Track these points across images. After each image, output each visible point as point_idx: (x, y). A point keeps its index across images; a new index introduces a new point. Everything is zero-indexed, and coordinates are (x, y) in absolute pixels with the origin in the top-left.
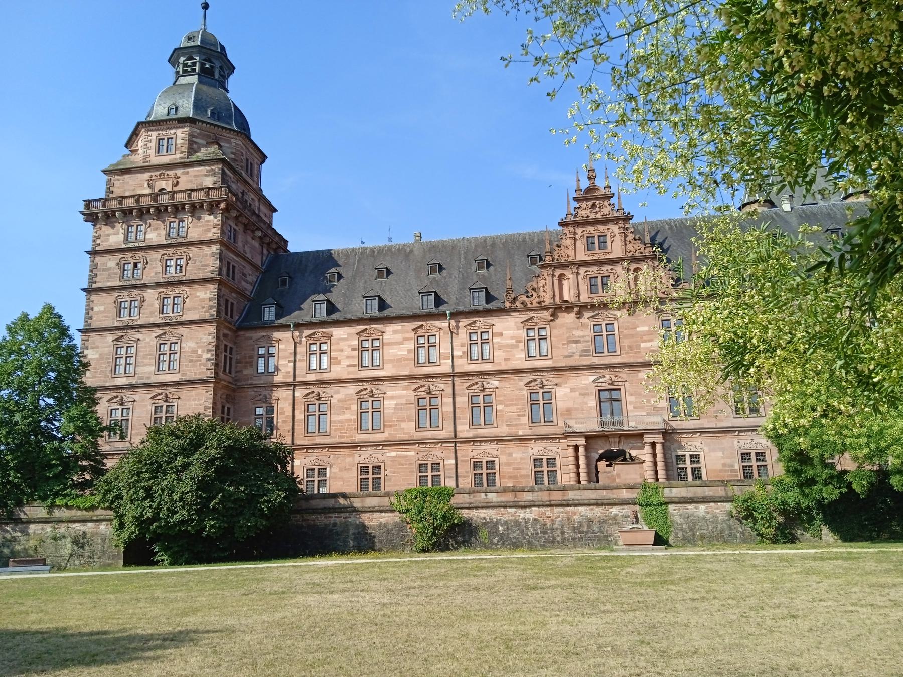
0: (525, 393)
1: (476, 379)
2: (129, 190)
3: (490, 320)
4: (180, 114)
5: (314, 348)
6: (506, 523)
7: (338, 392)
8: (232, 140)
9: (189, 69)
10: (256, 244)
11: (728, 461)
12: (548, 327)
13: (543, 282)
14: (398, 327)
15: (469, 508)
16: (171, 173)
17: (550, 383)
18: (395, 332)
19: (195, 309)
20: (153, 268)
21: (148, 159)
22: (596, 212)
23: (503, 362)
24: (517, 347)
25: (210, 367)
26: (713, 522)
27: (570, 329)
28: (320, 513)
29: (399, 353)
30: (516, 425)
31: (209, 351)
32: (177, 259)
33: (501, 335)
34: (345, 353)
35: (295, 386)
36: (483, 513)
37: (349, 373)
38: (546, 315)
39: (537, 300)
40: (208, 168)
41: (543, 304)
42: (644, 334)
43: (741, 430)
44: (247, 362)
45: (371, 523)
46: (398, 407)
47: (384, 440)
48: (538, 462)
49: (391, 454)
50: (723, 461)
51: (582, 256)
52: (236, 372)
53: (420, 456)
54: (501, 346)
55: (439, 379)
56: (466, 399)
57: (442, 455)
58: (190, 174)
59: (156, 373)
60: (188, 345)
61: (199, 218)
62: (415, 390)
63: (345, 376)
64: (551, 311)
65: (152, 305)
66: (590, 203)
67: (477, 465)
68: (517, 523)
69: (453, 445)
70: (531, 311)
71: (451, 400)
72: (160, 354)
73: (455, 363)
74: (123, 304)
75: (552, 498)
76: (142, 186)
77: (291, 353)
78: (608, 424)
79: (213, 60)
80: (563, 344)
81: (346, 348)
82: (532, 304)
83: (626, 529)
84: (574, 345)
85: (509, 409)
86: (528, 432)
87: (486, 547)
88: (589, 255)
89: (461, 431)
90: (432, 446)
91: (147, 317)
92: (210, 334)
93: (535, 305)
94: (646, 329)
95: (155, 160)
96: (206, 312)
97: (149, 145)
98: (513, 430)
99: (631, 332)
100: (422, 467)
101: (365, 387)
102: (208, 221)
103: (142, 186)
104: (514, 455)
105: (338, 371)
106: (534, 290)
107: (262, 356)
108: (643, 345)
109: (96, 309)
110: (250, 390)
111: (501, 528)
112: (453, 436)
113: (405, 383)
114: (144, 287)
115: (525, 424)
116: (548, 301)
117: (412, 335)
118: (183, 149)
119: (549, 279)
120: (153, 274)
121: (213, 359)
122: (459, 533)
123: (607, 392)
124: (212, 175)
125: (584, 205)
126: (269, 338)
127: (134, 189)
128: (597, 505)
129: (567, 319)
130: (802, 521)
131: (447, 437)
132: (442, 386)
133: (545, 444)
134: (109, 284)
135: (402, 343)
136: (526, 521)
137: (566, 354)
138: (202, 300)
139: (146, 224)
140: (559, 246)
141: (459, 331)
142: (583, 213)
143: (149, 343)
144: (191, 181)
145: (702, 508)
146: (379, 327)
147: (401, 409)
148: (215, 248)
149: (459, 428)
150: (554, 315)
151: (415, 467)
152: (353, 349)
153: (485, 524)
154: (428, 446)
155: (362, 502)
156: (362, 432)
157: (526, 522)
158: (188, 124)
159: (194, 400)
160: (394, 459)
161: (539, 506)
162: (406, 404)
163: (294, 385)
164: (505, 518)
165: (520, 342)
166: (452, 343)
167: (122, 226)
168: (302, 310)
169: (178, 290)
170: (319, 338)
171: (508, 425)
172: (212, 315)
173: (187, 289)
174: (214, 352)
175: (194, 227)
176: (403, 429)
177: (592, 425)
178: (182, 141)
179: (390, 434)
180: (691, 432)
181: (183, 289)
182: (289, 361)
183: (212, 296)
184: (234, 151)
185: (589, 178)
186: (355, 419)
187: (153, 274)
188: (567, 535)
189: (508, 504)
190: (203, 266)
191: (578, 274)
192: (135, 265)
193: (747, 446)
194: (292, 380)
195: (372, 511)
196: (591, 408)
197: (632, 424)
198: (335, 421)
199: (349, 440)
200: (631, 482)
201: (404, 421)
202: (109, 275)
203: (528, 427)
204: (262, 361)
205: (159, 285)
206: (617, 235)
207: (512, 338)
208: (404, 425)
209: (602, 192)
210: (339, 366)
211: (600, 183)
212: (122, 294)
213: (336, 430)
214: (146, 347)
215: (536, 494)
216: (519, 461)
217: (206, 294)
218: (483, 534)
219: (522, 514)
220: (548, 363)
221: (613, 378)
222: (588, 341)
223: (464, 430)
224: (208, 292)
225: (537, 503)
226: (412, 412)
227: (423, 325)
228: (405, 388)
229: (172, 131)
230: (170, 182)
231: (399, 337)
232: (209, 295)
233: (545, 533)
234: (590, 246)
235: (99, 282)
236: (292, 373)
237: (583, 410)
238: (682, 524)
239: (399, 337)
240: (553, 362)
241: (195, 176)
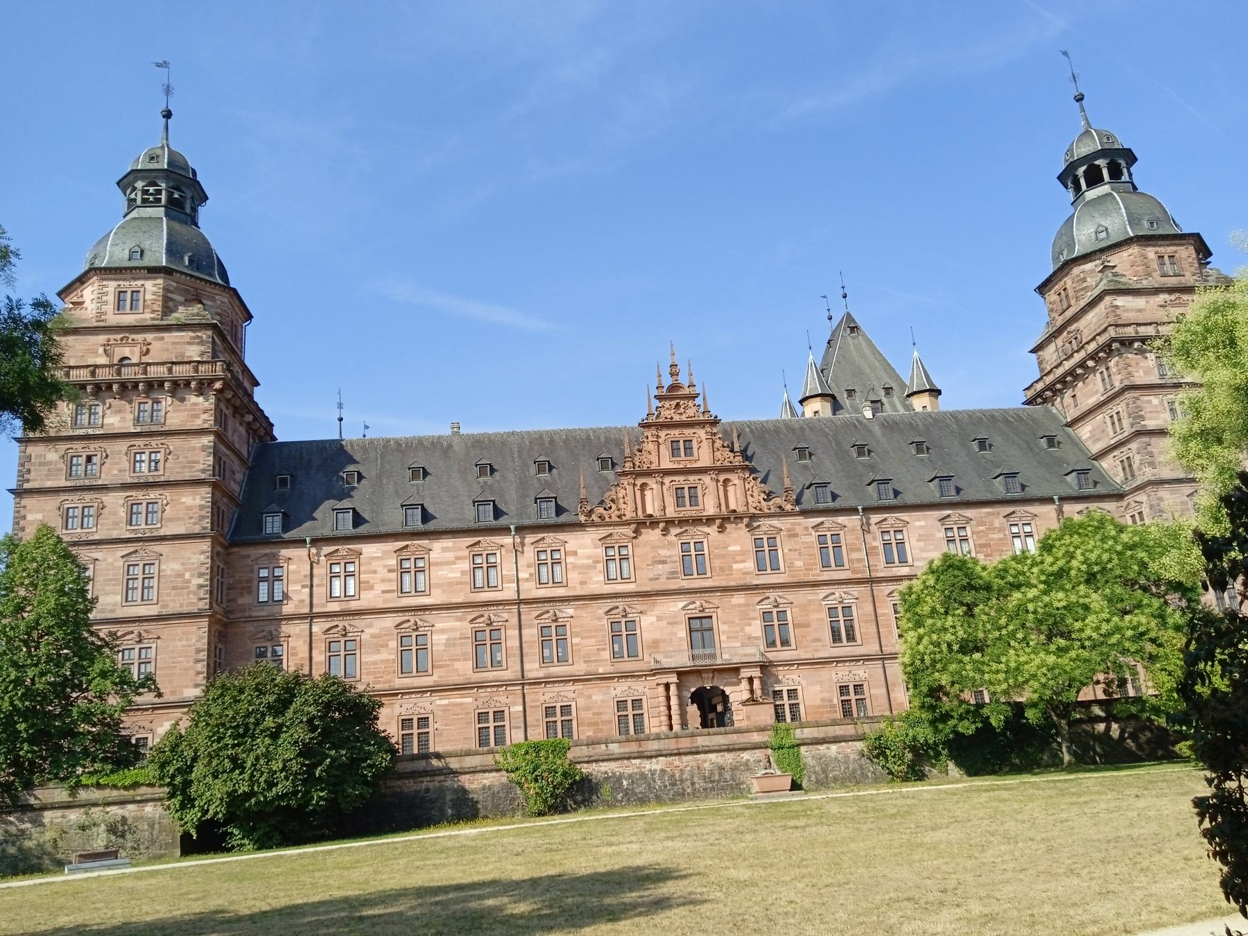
0: (605, 623)
1: (547, 607)
2: (75, 357)
3: (562, 536)
4: (149, 261)
5: (336, 569)
6: (630, 776)
7: (371, 626)
8: (217, 297)
9: (151, 198)
10: (242, 430)
11: (827, 695)
12: (630, 545)
13: (623, 491)
14: (448, 543)
15: (588, 762)
16: (139, 337)
17: (634, 611)
18: (445, 550)
19: (179, 519)
20: (116, 463)
21: (103, 317)
22: (681, 414)
23: (578, 586)
24: (595, 568)
25: (202, 596)
26: (845, 763)
27: (655, 548)
28: (407, 778)
29: (451, 575)
30: (596, 661)
31: (201, 575)
32: (151, 453)
33: (575, 553)
34: (379, 576)
35: (312, 618)
36: (605, 767)
37: (385, 601)
38: (628, 531)
39: (617, 513)
40: (191, 334)
41: (624, 518)
42: (736, 553)
43: (839, 661)
44: (242, 588)
45: (473, 786)
46: (450, 644)
47: (432, 684)
48: (622, 705)
49: (442, 701)
50: (821, 696)
51: (667, 464)
52: (229, 601)
53: (480, 703)
54: (575, 567)
55: (501, 607)
56: (535, 631)
57: (507, 701)
58: (166, 340)
59: (124, 604)
60: (170, 567)
61: (182, 400)
62: (472, 621)
63: (380, 605)
64: (633, 526)
65: (115, 514)
66: (674, 403)
67: (550, 711)
68: (643, 776)
69: (520, 687)
70: (610, 525)
71: (517, 632)
72: (128, 579)
73: (521, 588)
74: (71, 511)
75: (680, 746)
76: (95, 352)
77: (305, 576)
78: (699, 657)
79: (184, 189)
80: (648, 565)
81: (380, 569)
82: (610, 517)
83: (758, 775)
84: (660, 566)
85: (586, 642)
86: (610, 669)
87: (611, 806)
88: (674, 462)
89: (530, 671)
90: (494, 689)
91: (108, 529)
92: (203, 552)
93: (615, 519)
94: (737, 548)
95: (113, 319)
96: (195, 524)
97: (104, 298)
98: (592, 668)
99: (722, 552)
100: (482, 717)
101: (407, 618)
102: (195, 404)
103: (95, 352)
104: (594, 698)
105: (369, 599)
106: (613, 501)
107: (264, 579)
108: (735, 566)
109: (30, 517)
110: (248, 624)
111: (625, 783)
112: (520, 676)
113: (459, 613)
114: (104, 488)
115: (606, 660)
116: (629, 515)
117: (466, 553)
118: (155, 307)
119: (630, 488)
120: (116, 472)
121: (206, 586)
122: (577, 791)
123: (698, 621)
124: (198, 344)
125: (667, 404)
126: (275, 557)
127: (83, 356)
128: (729, 750)
129: (651, 536)
130: (930, 757)
131: (512, 678)
132: (506, 616)
133: (630, 683)
134: (49, 484)
135: (454, 563)
136: (653, 772)
137: (652, 576)
138: (189, 508)
139: (104, 404)
140: (640, 451)
141: (525, 548)
142: (666, 413)
143: (112, 564)
144: (167, 350)
145: (834, 748)
146: (425, 542)
147: (454, 645)
148: (208, 440)
149: (527, 666)
150: (637, 531)
151: (473, 717)
152: (390, 571)
153: (607, 779)
154: (489, 690)
155: (460, 761)
156: (404, 675)
157: (652, 775)
158: (162, 275)
159: (181, 640)
160: (445, 709)
161: (666, 756)
162: (460, 638)
163: (311, 617)
164: (629, 771)
165: (598, 562)
166: (516, 563)
167: (68, 406)
168: (314, 519)
169: (153, 494)
170: (343, 557)
171: (585, 662)
172: (205, 528)
173: (168, 494)
174: (208, 577)
175: (175, 411)
176: (457, 670)
177: (683, 660)
178: (154, 297)
179: (439, 677)
180: (789, 664)
181: (161, 492)
182: (303, 587)
183: (203, 502)
184: (219, 311)
185: (672, 375)
186: (393, 660)
187: (116, 472)
188: (697, 786)
189: (633, 755)
190: (188, 462)
191: (662, 483)
192: (89, 459)
193: (846, 678)
194: (307, 610)
195: (473, 771)
196: (680, 639)
197: (726, 656)
198: (367, 663)
199: (386, 686)
200: (762, 724)
201: (458, 660)
202: (49, 470)
203: (609, 663)
204: (264, 587)
205: (125, 487)
206: (704, 441)
207: (588, 557)
208: (457, 665)
209: (686, 391)
210: (372, 592)
211: (683, 379)
212: (70, 498)
213: (368, 674)
214: (107, 569)
215: (662, 741)
216: (599, 703)
217: (194, 499)
218: (606, 790)
219: (649, 766)
220: (631, 587)
221: (705, 605)
222: (676, 562)
223: (534, 669)
224: (198, 497)
225: (664, 753)
226: (469, 648)
227: (479, 542)
228: (459, 619)
229: (139, 283)
230: (137, 350)
231: (450, 556)
232: (198, 501)
233: (673, 784)
234: (675, 452)
235: (34, 480)
236: (308, 601)
237: (671, 641)
238: (814, 767)
239: (450, 556)
240: (637, 586)
241: (174, 343)
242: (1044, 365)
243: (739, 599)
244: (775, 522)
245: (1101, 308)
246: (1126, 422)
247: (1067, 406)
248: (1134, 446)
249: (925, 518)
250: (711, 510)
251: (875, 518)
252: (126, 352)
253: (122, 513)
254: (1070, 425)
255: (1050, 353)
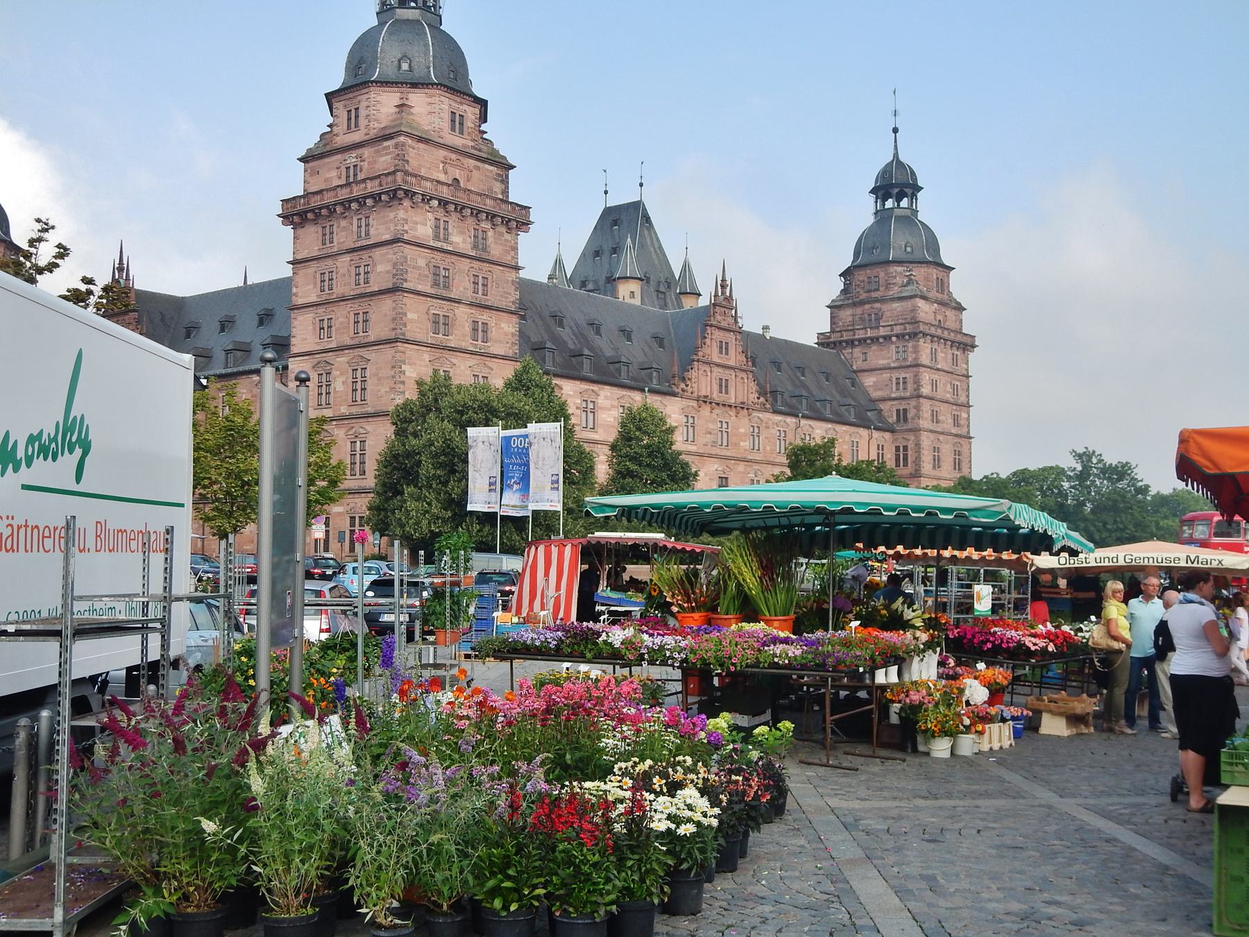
18: (606, 398)
19: (500, 342)
108: (742, 444)
109: (410, 316)
114: (458, 302)
117: (616, 403)
134: (420, 288)
152: (577, 408)
187: (462, 289)
235: (411, 281)
242: (836, 320)
243: (741, 467)
244: (761, 415)
245: (908, 304)
246: (910, 386)
247: (856, 357)
248: (913, 403)
249: (820, 428)
250: (732, 401)
251: (803, 422)
252: (457, 174)
253: (468, 328)
254: (855, 372)
255: (846, 315)
